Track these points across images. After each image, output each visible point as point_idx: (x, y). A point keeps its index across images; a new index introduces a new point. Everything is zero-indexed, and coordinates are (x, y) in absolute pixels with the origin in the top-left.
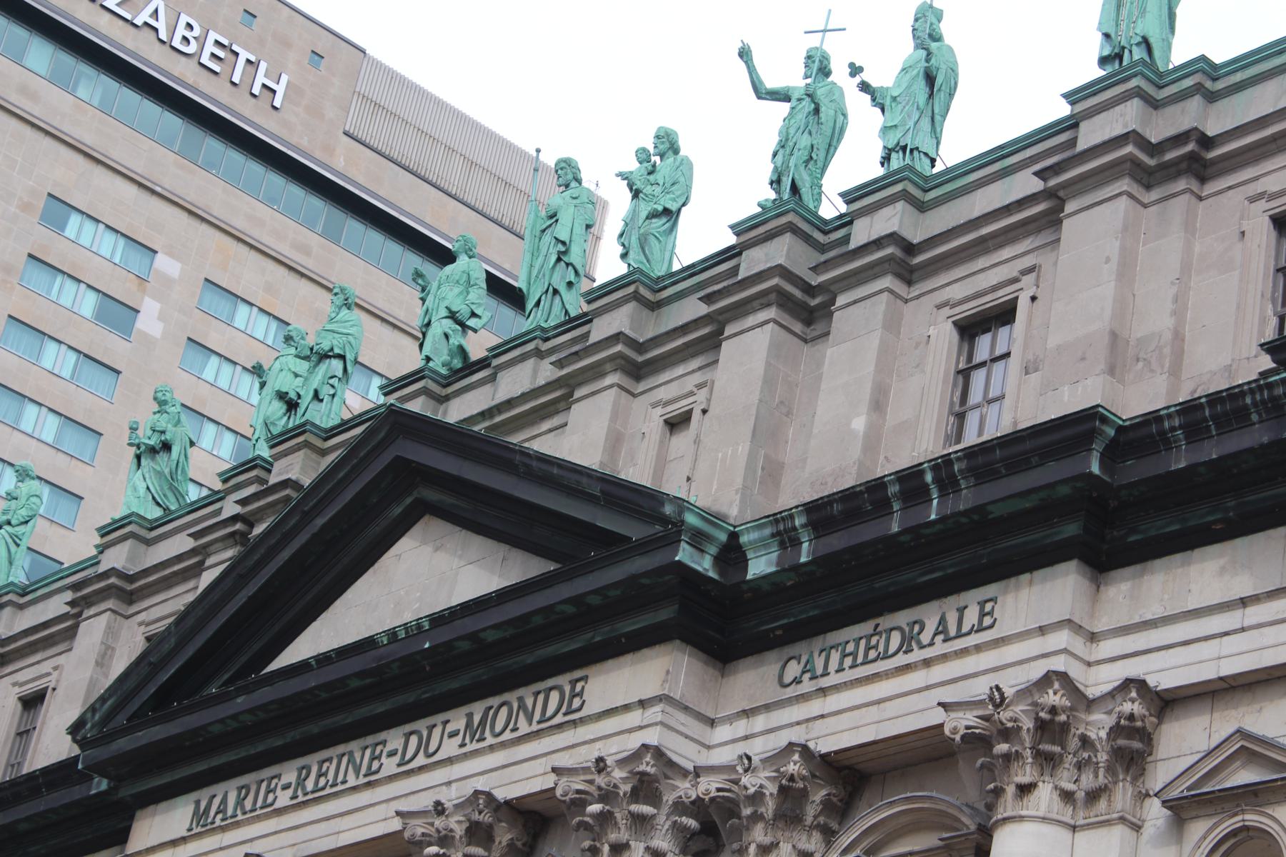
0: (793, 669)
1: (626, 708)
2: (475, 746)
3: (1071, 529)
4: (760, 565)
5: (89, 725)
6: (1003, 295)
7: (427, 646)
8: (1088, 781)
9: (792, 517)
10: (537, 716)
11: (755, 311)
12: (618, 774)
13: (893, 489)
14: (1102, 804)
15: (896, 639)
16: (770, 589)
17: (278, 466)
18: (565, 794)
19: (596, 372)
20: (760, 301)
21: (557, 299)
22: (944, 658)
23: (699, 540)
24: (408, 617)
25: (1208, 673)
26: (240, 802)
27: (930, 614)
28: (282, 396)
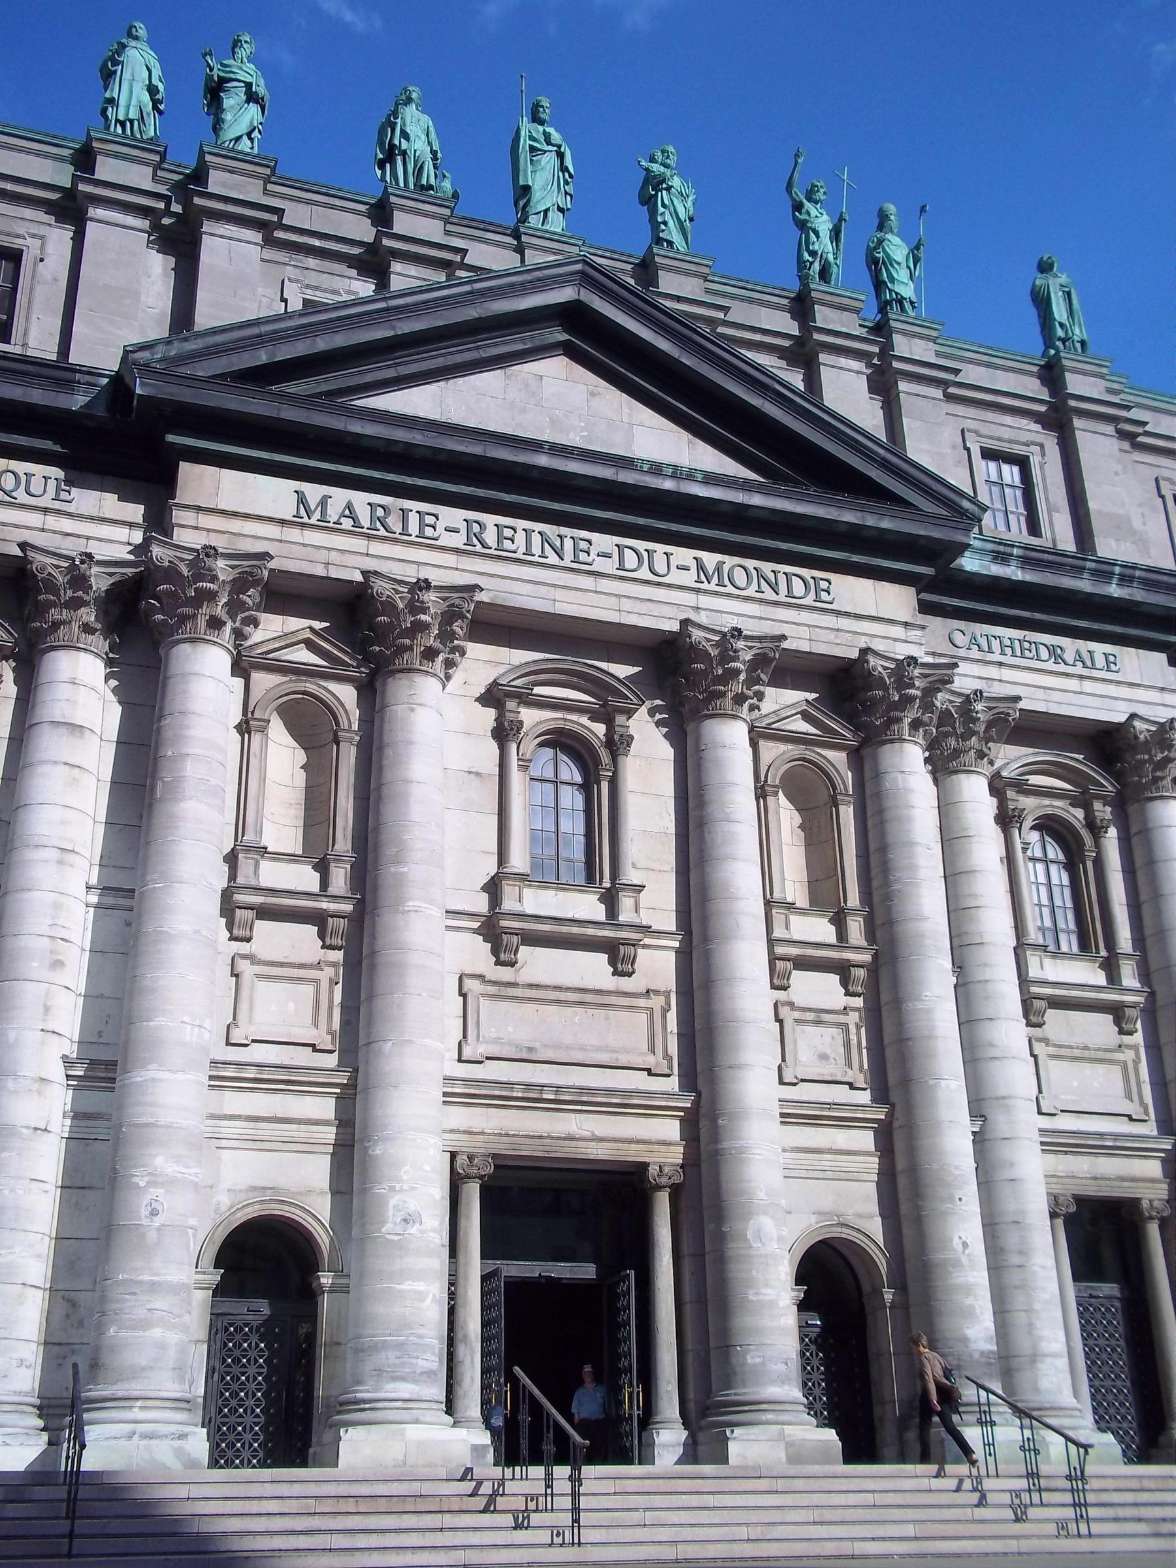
0: (959, 638)
2: (712, 587)
6: (1020, 450)
15: (1044, 653)
27: (1069, 645)
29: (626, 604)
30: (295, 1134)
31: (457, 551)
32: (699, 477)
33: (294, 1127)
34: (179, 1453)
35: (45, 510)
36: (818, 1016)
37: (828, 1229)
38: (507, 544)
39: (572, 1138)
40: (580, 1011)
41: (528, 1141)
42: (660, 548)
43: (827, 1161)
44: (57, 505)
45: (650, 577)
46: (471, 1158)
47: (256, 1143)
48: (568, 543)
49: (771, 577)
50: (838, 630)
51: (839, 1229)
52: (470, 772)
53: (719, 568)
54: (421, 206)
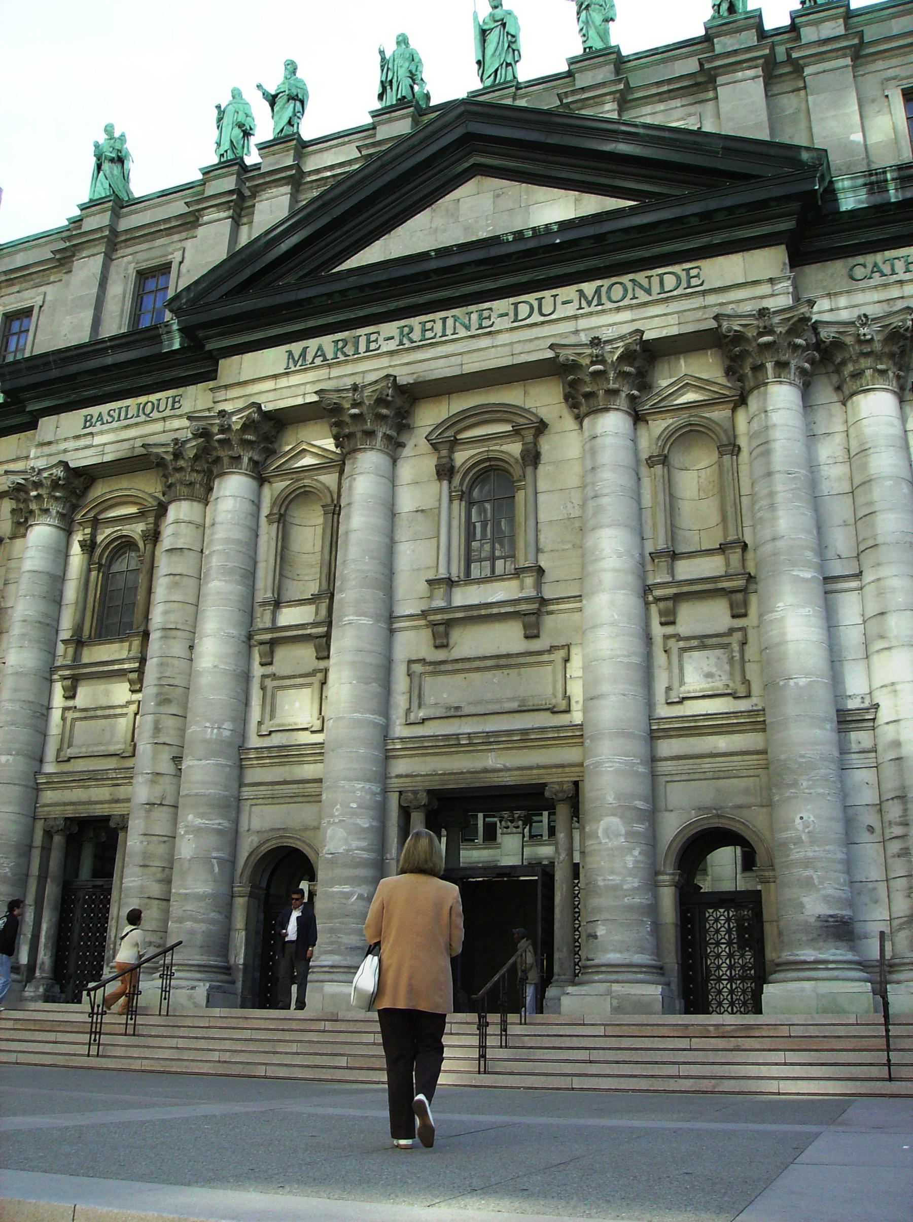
0: (859, 272)
1: (756, 283)
2: (593, 309)
4: (848, 202)
5: (184, 300)
7: (558, 241)
9: (885, 173)
10: (656, 288)
11: (743, 70)
12: (776, 320)
18: (729, 331)
21: (510, 68)
28: (240, 125)
30: (297, 791)
32: (555, 228)
33: (295, 786)
34: (190, 997)
35: (164, 419)
37: (706, 822)
38: (429, 334)
39: (486, 771)
40: (498, 673)
41: (453, 777)
42: (547, 294)
44: (172, 413)
45: (542, 319)
46: (415, 793)
47: (274, 799)
48: (474, 317)
49: (645, 283)
50: (705, 307)
51: (717, 821)
52: (417, 511)
53: (598, 291)
54: (393, 114)
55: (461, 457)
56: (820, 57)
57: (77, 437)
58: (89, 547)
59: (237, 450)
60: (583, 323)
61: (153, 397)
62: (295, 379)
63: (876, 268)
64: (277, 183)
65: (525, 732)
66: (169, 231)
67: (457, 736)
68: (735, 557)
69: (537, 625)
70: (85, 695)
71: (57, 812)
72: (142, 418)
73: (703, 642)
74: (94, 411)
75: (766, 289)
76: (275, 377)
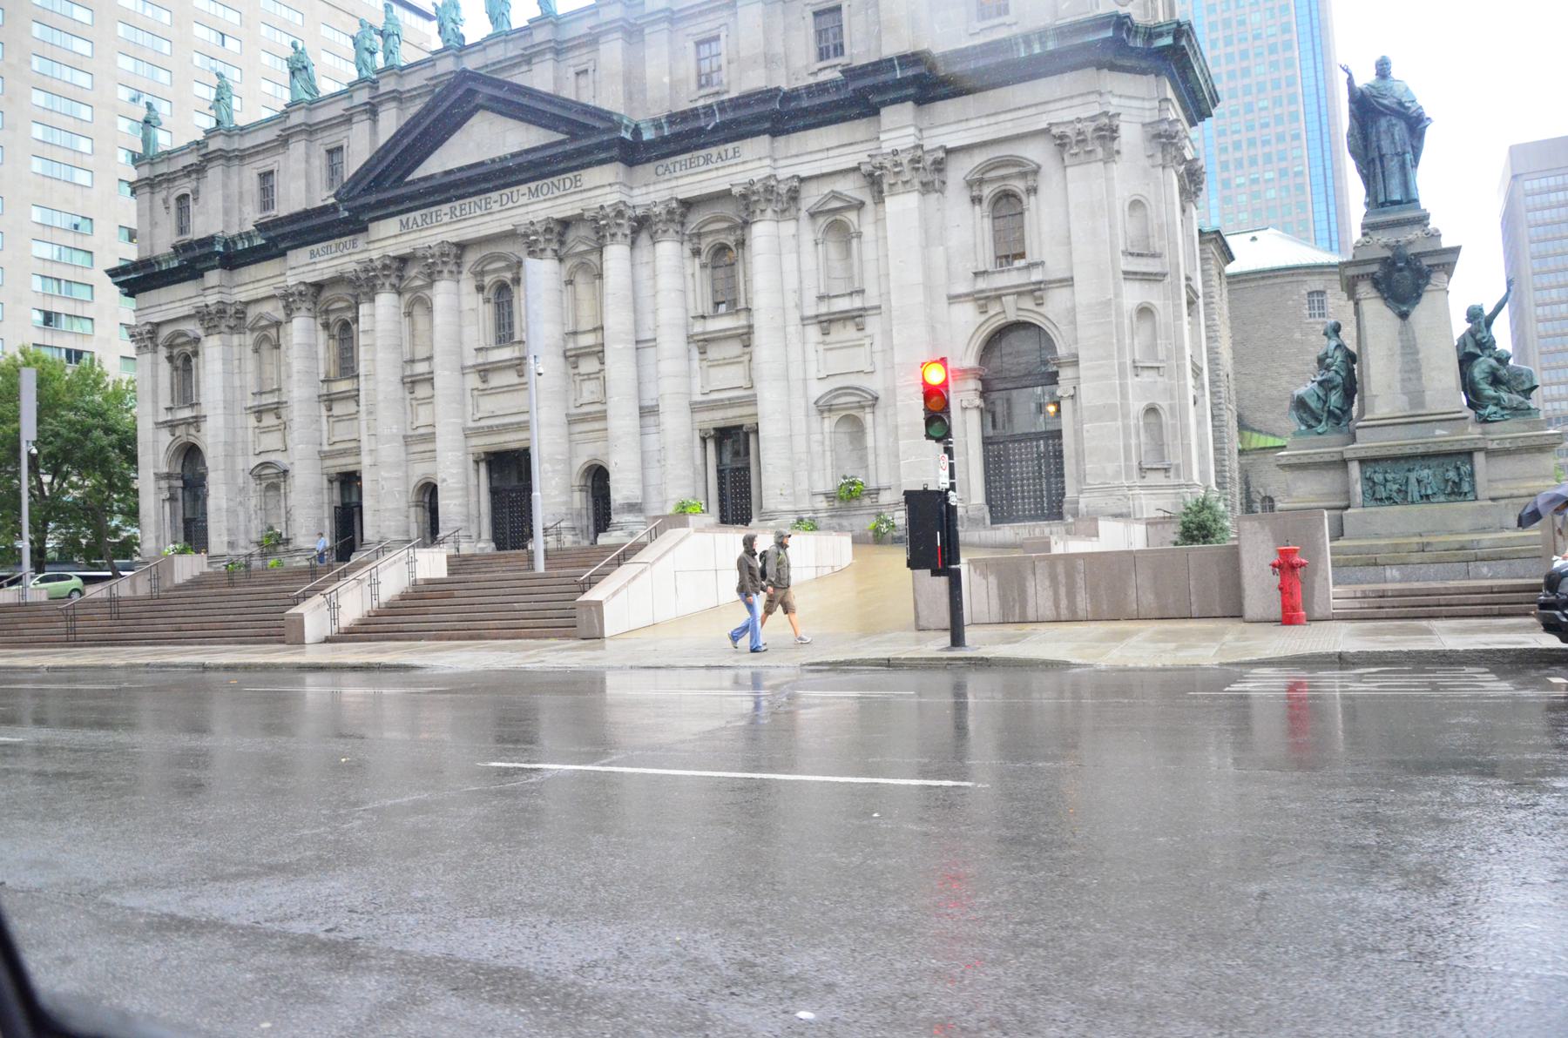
0: (661, 170)
3: (767, 125)
4: (648, 135)
6: (714, 33)
8: (779, 207)
13: (701, 111)
14: (787, 214)
16: (650, 145)
17: (381, 82)
19: (541, 53)
20: (614, 30)
22: (723, 167)
23: (627, 127)
24: (501, 154)
25: (817, 172)
26: (423, 220)
27: (714, 151)
29: (504, 222)
31: (446, 224)
36: (589, 377)
43: (591, 435)
55: (488, 280)
56: (654, 23)
57: (308, 265)
58: (326, 326)
59: (383, 280)
60: (531, 208)
61: (344, 239)
62: (405, 238)
63: (667, 168)
64: (388, 100)
65: (518, 423)
66: (338, 124)
67: (492, 427)
68: (599, 334)
69: (522, 371)
70: (339, 409)
71: (334, 471)
72: (339, 254)
73: (589, 377)
74: (315, 247)
75: (608, 189)
76: (395, 236)
